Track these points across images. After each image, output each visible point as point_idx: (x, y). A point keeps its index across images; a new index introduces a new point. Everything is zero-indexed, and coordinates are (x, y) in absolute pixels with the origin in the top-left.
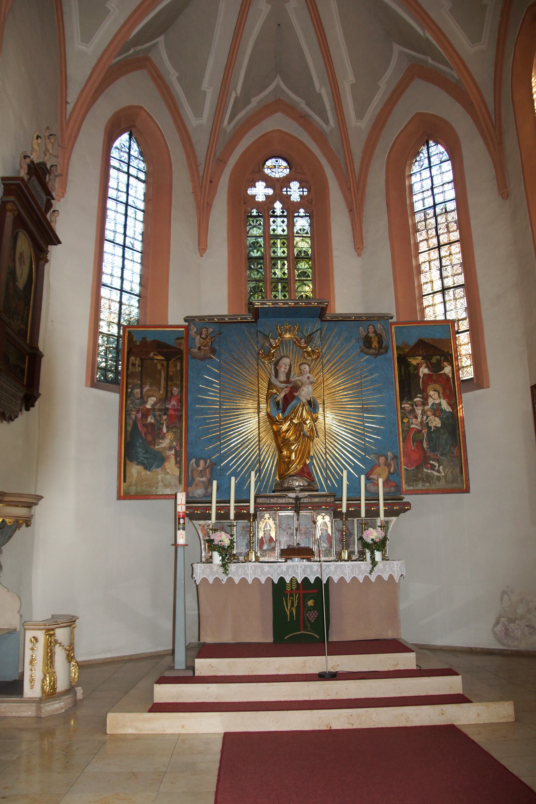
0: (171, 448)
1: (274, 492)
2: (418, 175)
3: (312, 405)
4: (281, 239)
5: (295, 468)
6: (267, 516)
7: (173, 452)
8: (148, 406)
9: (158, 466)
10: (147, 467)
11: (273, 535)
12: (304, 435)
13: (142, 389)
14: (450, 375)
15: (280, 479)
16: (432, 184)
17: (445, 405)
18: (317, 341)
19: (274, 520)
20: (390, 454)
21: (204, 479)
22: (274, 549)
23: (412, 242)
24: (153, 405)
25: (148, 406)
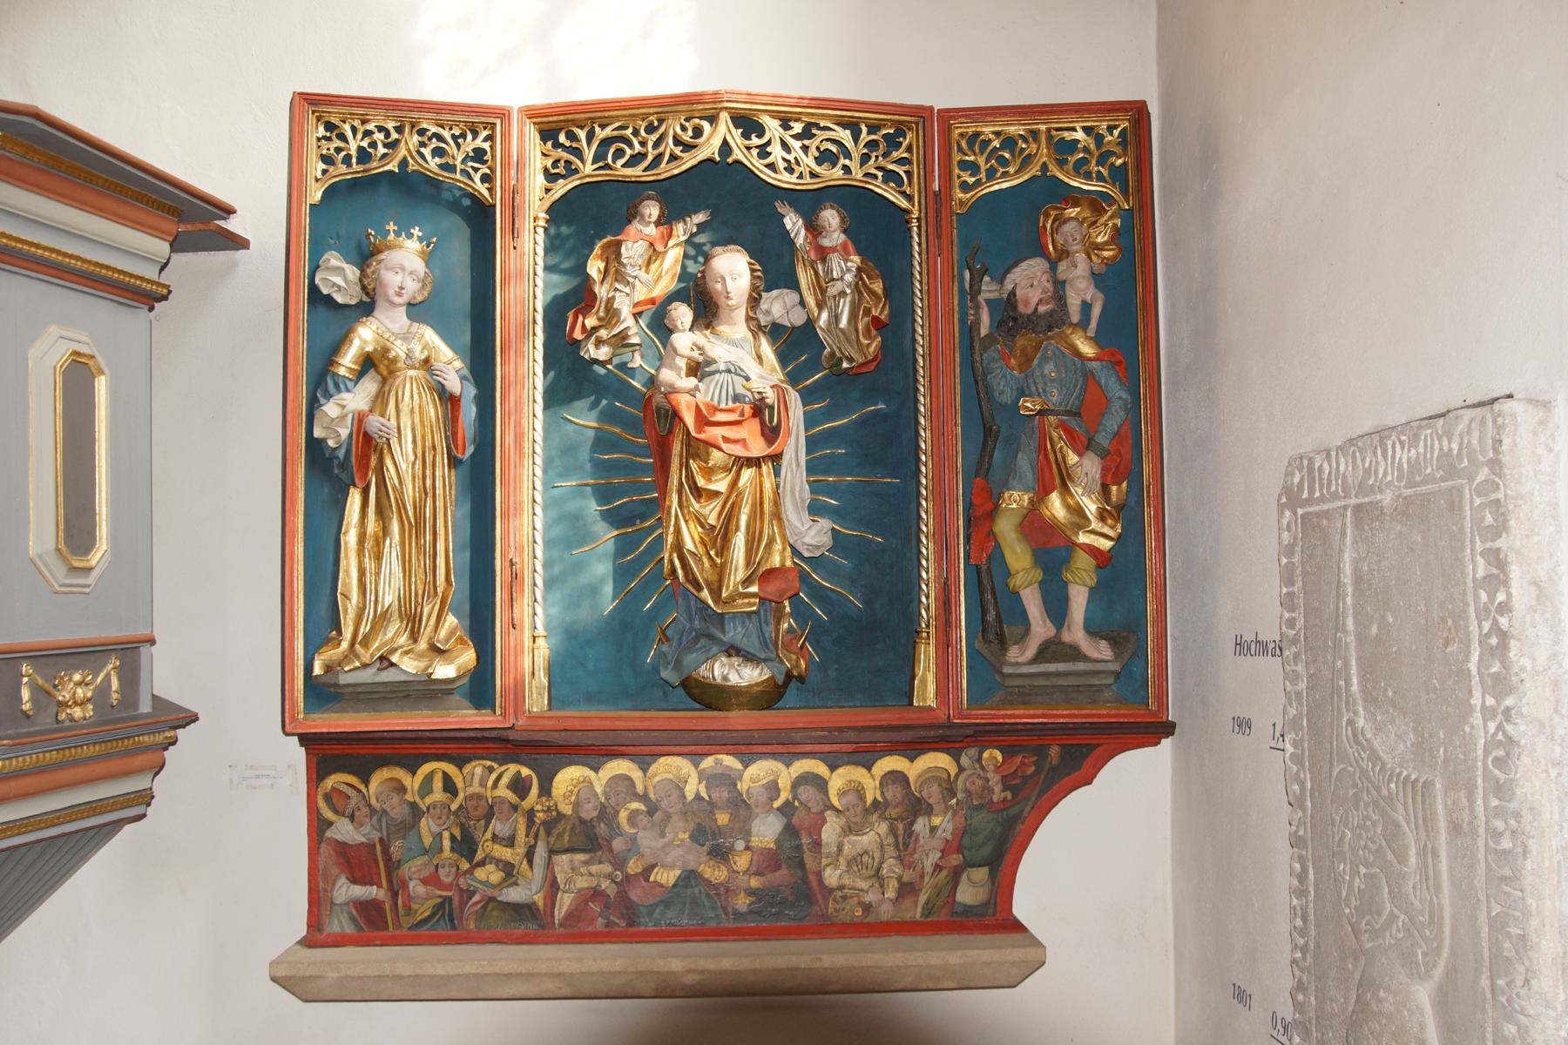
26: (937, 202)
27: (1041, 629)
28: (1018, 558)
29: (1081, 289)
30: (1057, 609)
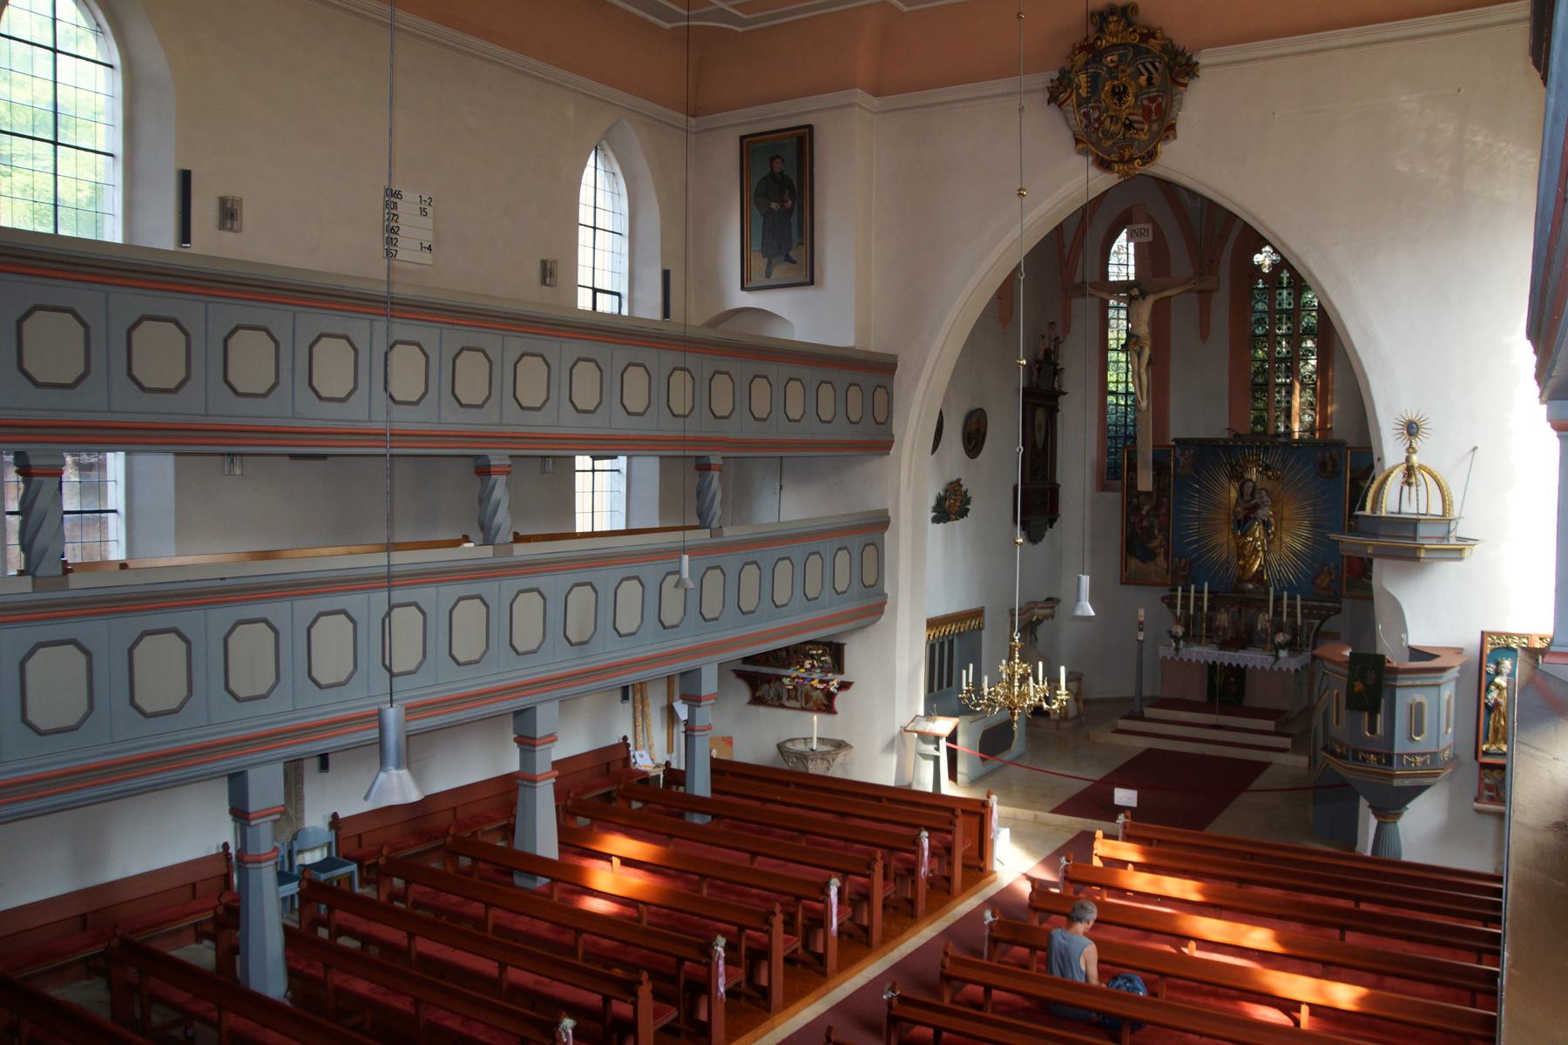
0: (1160, 547)
6: (1223, 610)
7: (1163, 550)
8: (1144, 513)
9: (1151, 560)
10: (1143, 561)
11: (1226, 624)
19: (1228, 614)
20: (1332, 565)
21: (1184, 573)
24: (1147, 513)
25: (1144, 513)
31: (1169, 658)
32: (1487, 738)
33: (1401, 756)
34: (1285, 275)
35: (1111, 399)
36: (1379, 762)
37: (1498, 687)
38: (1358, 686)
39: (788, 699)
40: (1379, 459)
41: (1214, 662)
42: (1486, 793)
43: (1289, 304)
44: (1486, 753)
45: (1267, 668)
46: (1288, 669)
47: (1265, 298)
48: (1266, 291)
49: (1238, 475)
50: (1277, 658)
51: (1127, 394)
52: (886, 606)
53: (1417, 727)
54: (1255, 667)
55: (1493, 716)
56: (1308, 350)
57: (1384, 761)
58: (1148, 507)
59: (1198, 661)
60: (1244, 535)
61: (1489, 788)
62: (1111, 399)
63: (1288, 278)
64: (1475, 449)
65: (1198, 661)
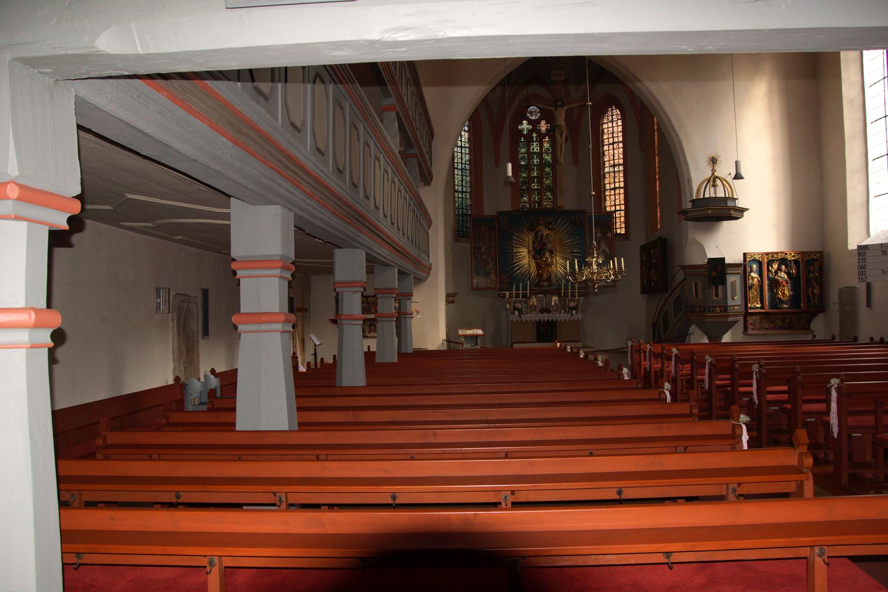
1: (536, 287)
2: (607, 125)
3: (551, 252)
4: (536, 155)
5: (545, 276)
6: (533, 297)
7: (493, 270)
11: (536, 304)
12: (548, 265)
13: (479, 244)
14: (610, 237)
15: (538, 281)
16: (613, 131)
17: (607, 250)
18: (553, 223)
19: (536, 298)
22: (536, 309)
23: (601, 161)
24: (484, 251)
26: (803, 260)
27: (813, 301)
28: (811, 295)
29: (816, 269)
30: (814, 300)
31: (515, 320)
32: (750, 302)
33: (730, 306)
34: (535, 135)
35: (456, 194)
36: (721, 310)
37: (753, 278)
38: (714, 274)
39: (369, 332)
40: (688, 180)
41: (540, 320)
42: (751, 327)
43: (537, 150)
44: (751, 308)
45: (567, 320)
46: (578, 320)
47: (525, 146)
48: (525, 143)
49: (532, 229)
50: (572, 314)
51: (462, 192)
52: (431, 271)
53: (734, 294)
54: (561, 320)
55: (751, 291)
56: (547, 173)
57: (723, 310)
58: (485, 248)
59: (531, 320)
60: (541, 258)
61: (752, 324)
62: (456, 194)
63: (536, 137)
64: (730, 174)
65: (531, 320)
